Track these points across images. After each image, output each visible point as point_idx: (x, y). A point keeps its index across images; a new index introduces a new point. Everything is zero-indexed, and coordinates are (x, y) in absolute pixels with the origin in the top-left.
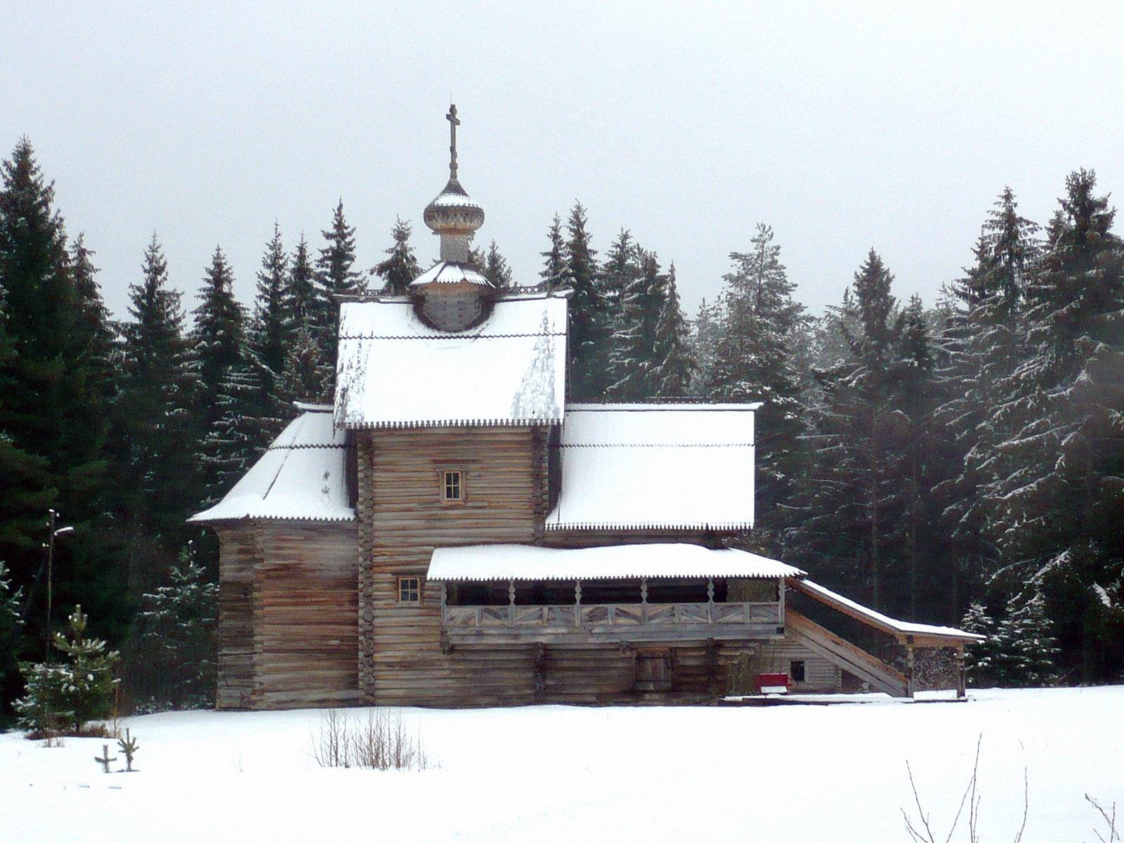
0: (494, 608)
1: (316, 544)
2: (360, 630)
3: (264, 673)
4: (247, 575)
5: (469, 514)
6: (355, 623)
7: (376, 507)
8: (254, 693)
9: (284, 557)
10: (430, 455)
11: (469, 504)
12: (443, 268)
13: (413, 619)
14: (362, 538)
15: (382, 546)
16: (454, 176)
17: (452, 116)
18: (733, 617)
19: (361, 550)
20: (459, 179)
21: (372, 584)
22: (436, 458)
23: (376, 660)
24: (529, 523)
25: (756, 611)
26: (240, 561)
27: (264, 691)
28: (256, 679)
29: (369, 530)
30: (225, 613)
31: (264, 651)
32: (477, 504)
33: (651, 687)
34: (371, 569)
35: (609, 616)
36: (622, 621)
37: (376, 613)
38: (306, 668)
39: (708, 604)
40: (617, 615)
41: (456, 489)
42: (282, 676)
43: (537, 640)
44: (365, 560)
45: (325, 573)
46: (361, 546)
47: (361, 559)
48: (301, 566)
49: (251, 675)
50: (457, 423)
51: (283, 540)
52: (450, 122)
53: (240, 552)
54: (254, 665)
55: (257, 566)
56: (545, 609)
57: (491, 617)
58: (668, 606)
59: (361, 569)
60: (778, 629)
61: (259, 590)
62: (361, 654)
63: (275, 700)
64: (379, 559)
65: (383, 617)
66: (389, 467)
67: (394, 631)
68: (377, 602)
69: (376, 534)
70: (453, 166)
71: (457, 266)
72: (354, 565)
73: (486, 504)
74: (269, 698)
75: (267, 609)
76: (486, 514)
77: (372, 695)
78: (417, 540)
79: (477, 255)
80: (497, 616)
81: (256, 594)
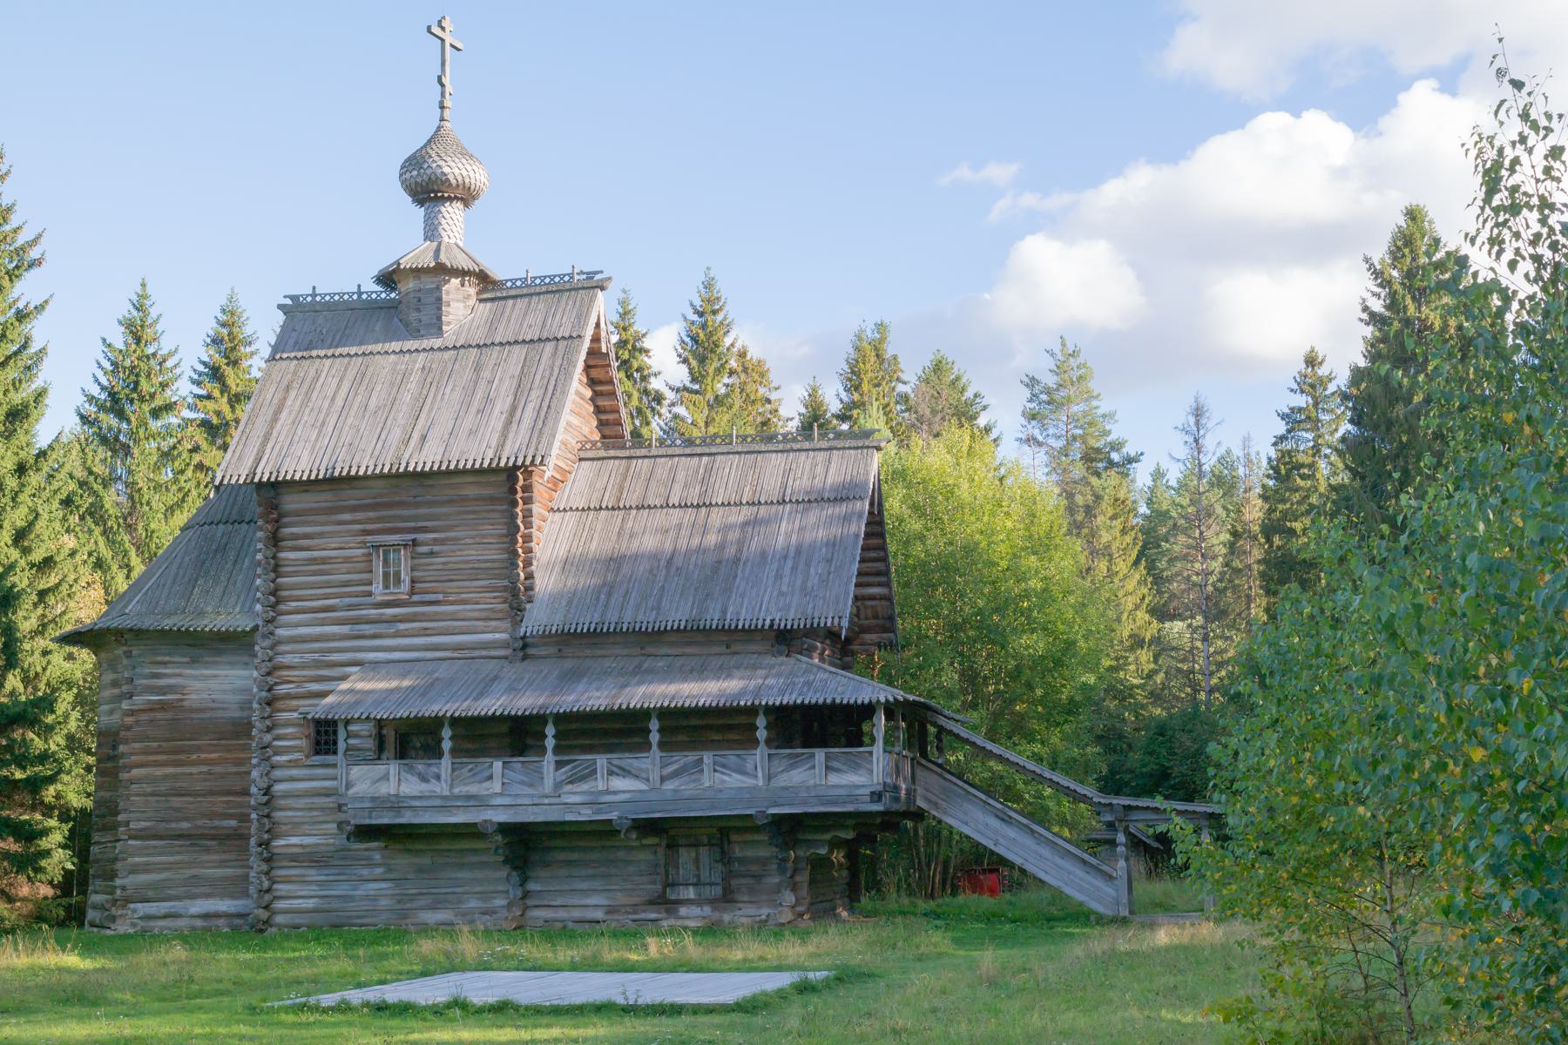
0: (420, 766)
1: (206, 668)
2: (253, 802)
5: (415, 614)
6: (246, 793)
7: (282, 607)
11: (416, 598)
15: (289, 667)
19: (255, 674)
21: (269, 730)
23: (276, 851)
25: (835, 764)
27: (128, 901)
28: (118, 882)
29: (266, 643)
36: (618, 783)
37: (277, 773)
38: (190, 865)
39: (758, 752)
40: (611, 773)
41: (397, 574)
42: (154, 877)
43: (487, 818)
45: (220, 714)
48: (185, 703)
54: (116, 859)
55: (125, 705)
56: (498, 765)
57: (414, 779)
58: (692, 757)
60: (873, 793)
61: (126, 742)
63: (141, 914)
64: (283, 689)
66: (316, 542)
67: (303, 802)
68: (278, 758)
73: (440, 597)
74: (134, 911)
75: (136, 772)
76: (442, 613)
77: (266, 907)
78: (335, 657)
80: (424, 779)
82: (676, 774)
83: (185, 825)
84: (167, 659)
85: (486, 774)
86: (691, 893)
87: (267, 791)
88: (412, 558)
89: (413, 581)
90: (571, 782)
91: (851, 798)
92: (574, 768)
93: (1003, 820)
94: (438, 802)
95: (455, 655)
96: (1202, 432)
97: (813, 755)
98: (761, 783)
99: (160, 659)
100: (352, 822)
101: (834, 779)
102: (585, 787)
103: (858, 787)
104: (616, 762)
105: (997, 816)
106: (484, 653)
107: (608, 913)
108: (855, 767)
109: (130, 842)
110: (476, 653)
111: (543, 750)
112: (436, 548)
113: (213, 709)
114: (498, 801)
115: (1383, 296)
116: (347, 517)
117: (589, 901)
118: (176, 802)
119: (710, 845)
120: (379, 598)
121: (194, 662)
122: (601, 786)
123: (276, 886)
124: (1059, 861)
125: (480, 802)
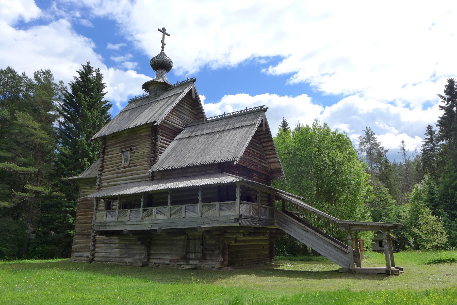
5: (130, 170)
10: (120, 146)
11: (130, 165)
16: (163, 50)
20: (165, 51)
36: (159, 217)
39: (199, 204)
60: (235, 219)
78: (112, 183)
82: (175, 213)
83: (86, 231)
84: (86, 187)
85: (126, 215)
86: (193, 256)
88: (131, 154)
89: (130, 161)
90: (146, 217)
91: (229, 221)
92: (148, 212)
93: (305, 230)
94: (114, 224)
95: (138, 181)
96: (404, 146)
97: (215, 205)
99: (85, 187)
100: (96, 230)
101: (223, 213)
102: (150, 218)
103: (230, 216)
104: (158, 209)
105: (302, 229)
106: (144, 179)
107: (170, 262)
108: (230, 208)
109: (76, 236)
110: (142, 180)
111: (140, 207)
112: (136, 151)
114: (128, 223)
115: (445, 101)
116: (118, 145)
118: (85, 225)
119: (199, 239)
120: (123, 166)
121: (91, 188)
122: (154, 218)
123: (96, 249)
124: (325, 246)
125: (123, 223)
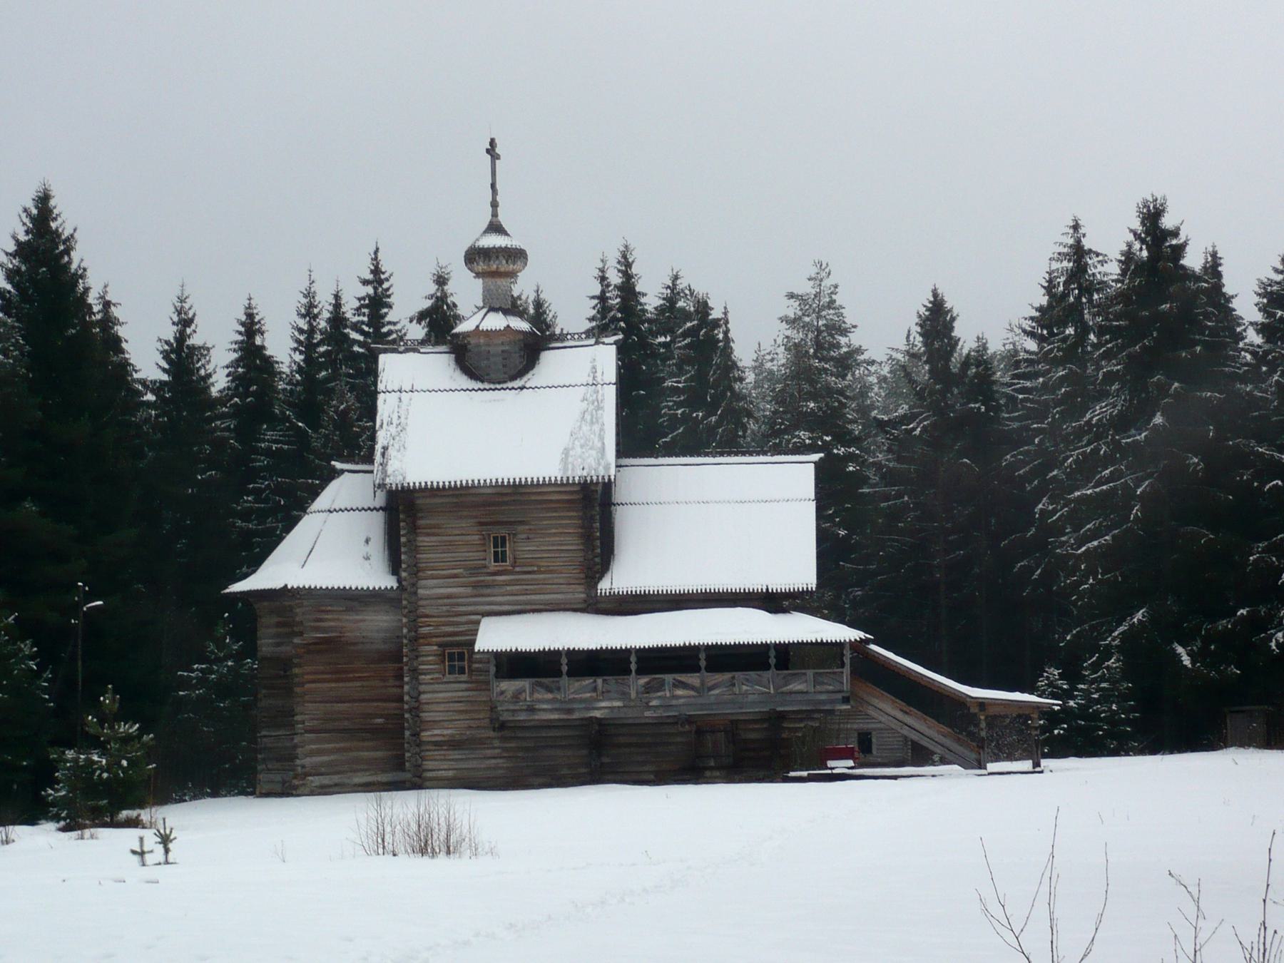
0: (546, 681)
1: (357, 615)
2: (406, 707)
3: (306, 756)
4: (286, 649)
6: (400, 699)
7: (420, 574)
8: (295, 777)
9: (324, 630)
10: (476, 517)
11: (517, 569)
12: (485, 315)
13: (460, 694)
14: (405, 608)
15: (427, 616)
16: (495, 215)
17: (492, 150)
18: (797, 686)
19: (405, 620)
22: (482, 520)
23: (424, 739)
24: (581, 588)
25: (821, 679)
26: (278, 635)
28: (298, 762)
29: (413, 599)
30: (264, 691)
31: (307, 731)
32: (525, 569)
33: (712, 764)
34: (416, 641)
35: (667, 687)
36: (679, 692)
37: (422, 688)
38: (350, 749)
39: (770, 672)
40: (675, 686)
41: (504, 553)
42: (325, 758)
43: (591, 715)
44: (409, 631)
46: (405, 616)
47: (405, 631)
48: (342, 639)
49: (293, 758)
50: (503, 482)
51: (323, 611)
52: (489, 157)
53: (279, 625)
55: (297, 640)
56: (600, 681)
58: (727, 676)
59: (405, 641)
60: (843, 697)
61: (299, 665)
62: (407, 733)
63: (317, 784)
65: (429, 692)
66: (433, 530)
67: (442, 707)
68: (423, 677)
69: (421, 603)
70: (494, 205)
71: (500, 312)
72: (398, 637)
73: (536, 569)
74: (312, 782)
75: (307, 686)
77: (420, 777)
79: (520, 299)
80: (549, 690)
81: (296, 671)
87: (417, 699)
98: (772, 692)
109: (306, 735)
113: (363, 643)
117: (646, 768)
